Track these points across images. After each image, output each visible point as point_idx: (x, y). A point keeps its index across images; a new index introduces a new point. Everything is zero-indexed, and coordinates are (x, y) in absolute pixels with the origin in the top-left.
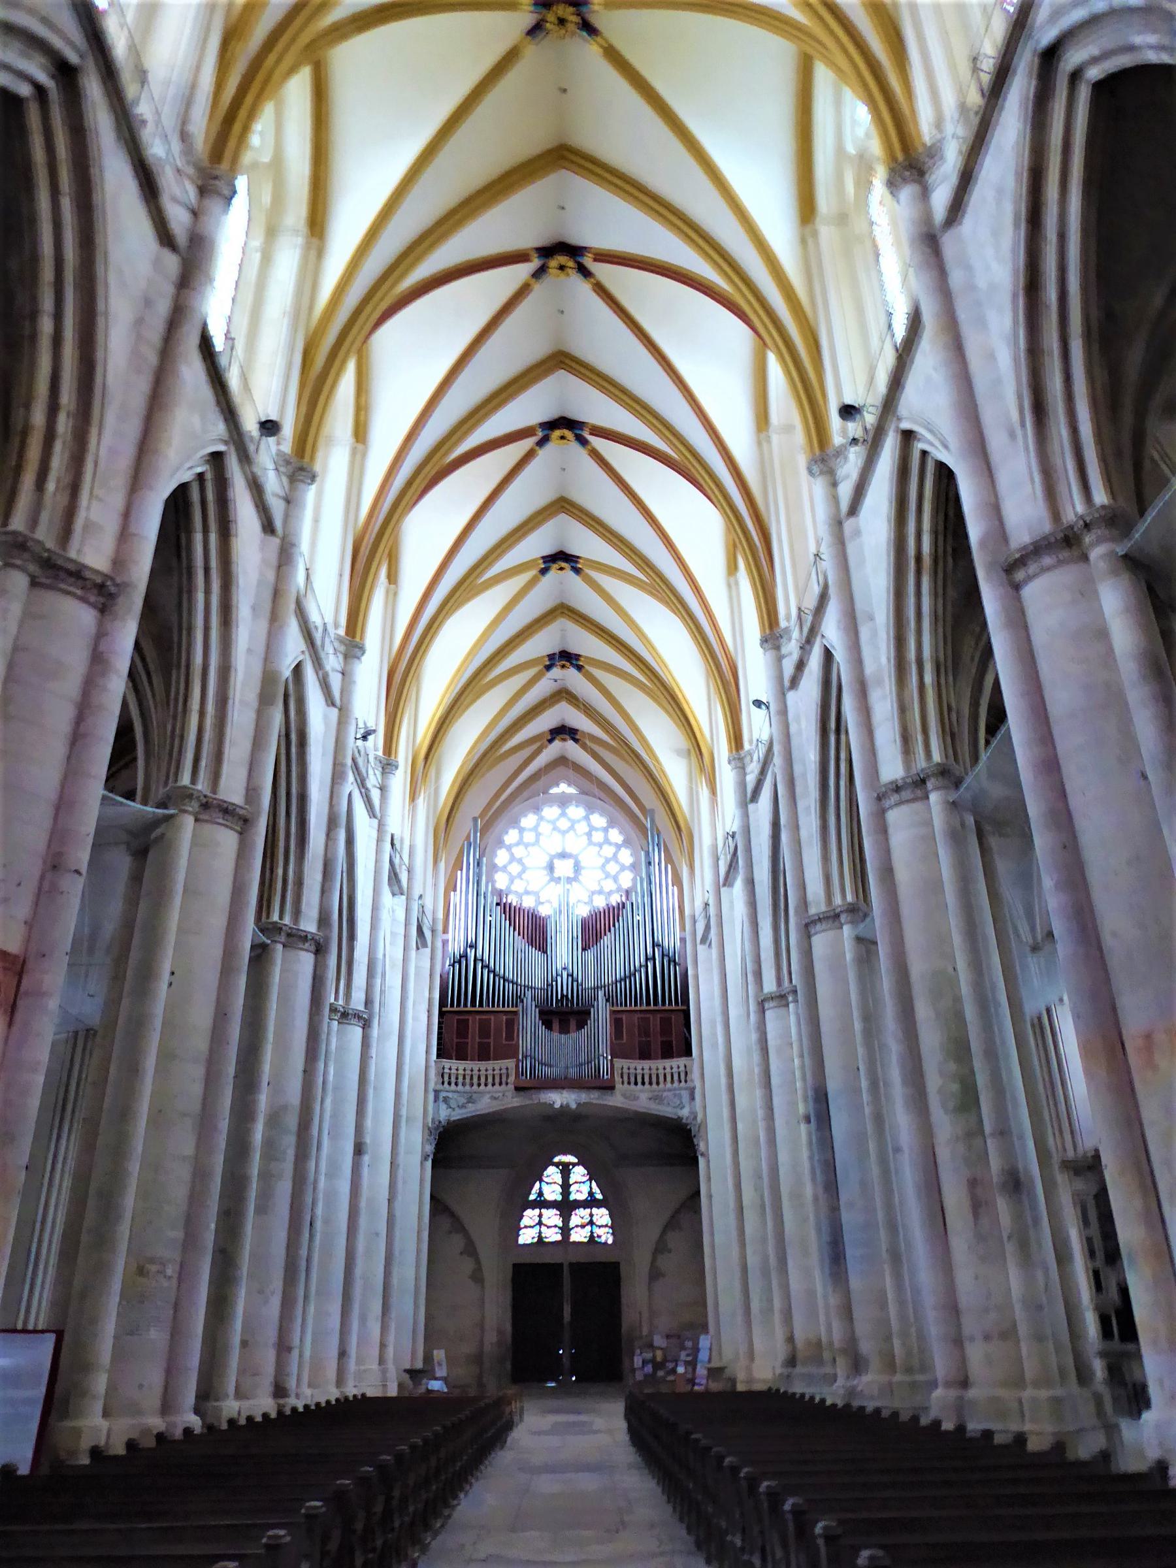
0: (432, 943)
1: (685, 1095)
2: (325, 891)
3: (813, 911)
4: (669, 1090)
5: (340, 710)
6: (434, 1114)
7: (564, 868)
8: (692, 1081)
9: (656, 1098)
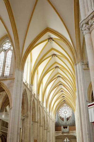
2: (47, 126)
7: (65, 112)
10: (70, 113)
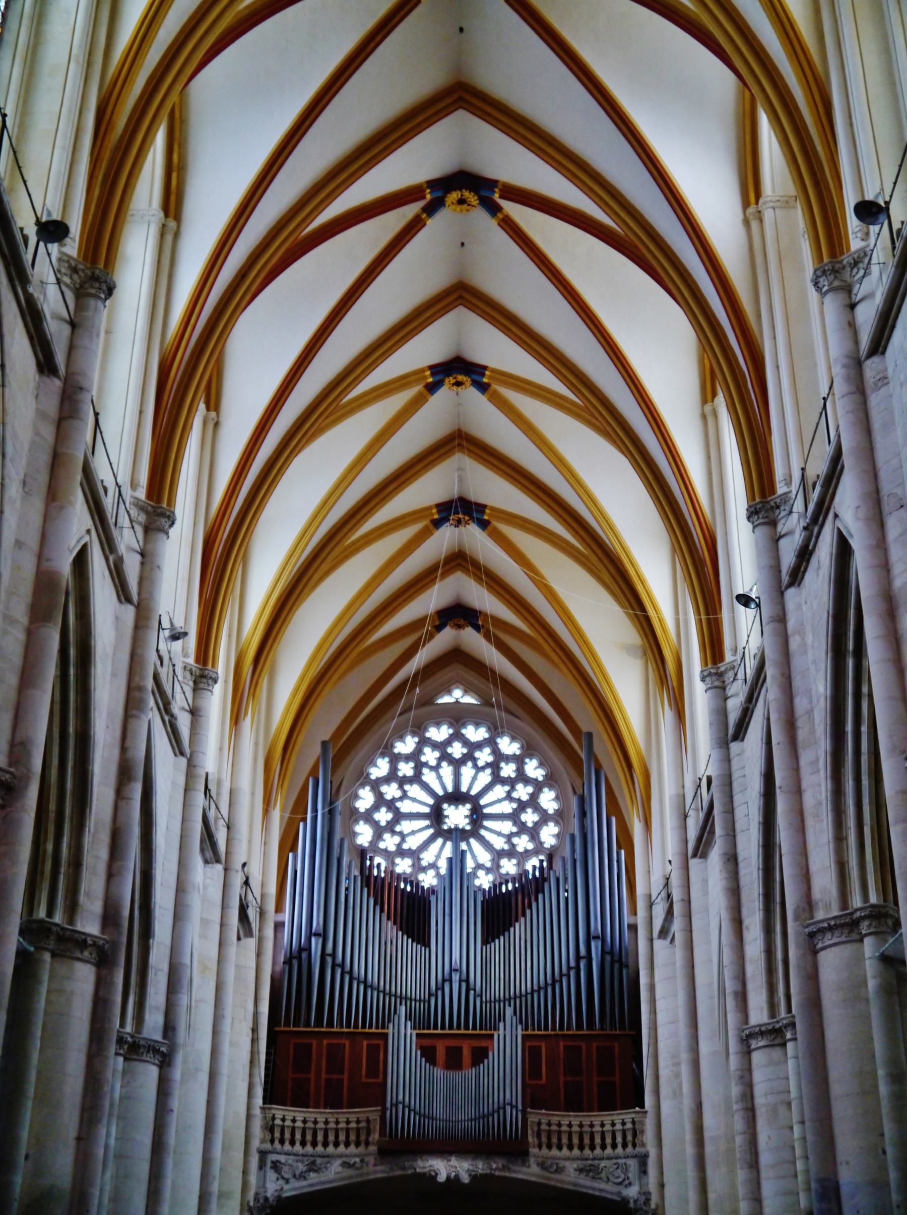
0: (260, 930)
1: (633, 1164)
2: (112, 875)
3: (820, 915)
4: (609, 1158)
5: (138, 607)
6: (258, 1187)
8: (643, 1145)
9: (591, 1171)
10: (534, 833)
